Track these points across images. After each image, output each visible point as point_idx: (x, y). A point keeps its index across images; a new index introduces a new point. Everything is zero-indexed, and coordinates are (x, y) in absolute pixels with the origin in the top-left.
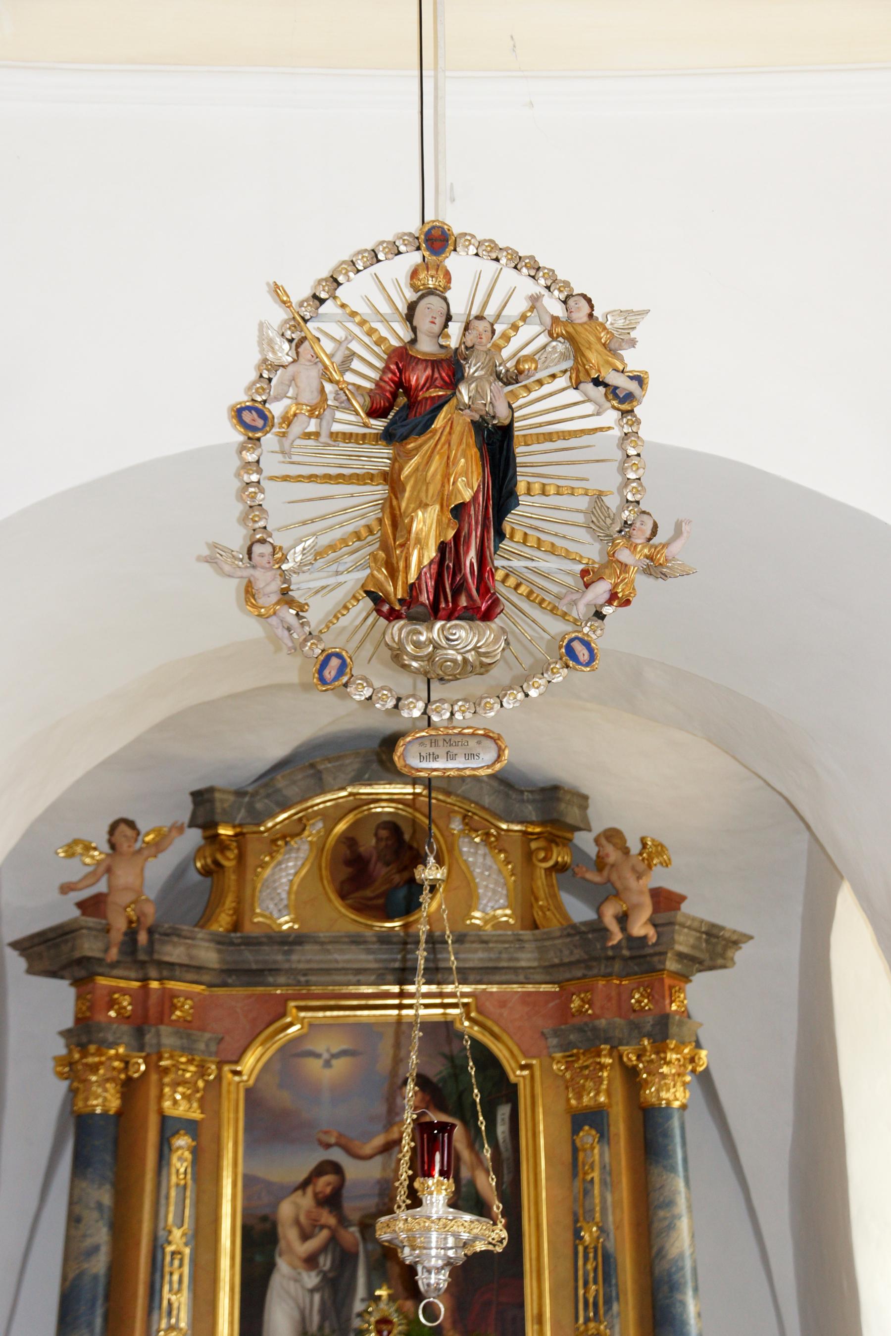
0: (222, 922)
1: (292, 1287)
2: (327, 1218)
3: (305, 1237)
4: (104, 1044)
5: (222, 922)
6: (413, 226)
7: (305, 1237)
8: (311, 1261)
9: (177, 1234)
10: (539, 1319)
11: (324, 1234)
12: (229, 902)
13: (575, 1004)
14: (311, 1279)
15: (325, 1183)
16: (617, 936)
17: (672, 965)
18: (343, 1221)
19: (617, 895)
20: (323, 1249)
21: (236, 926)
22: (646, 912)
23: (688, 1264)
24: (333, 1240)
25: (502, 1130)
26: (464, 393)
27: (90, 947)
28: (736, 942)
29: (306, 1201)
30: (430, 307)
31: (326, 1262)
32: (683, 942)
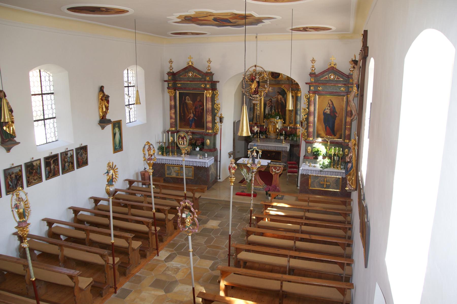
1: (268, 108)
3: (269, 104)
6: (254, 65)
7: (269, 104)
8: (269, 106)
10: (287, 112)
14: (269, 108)
15: (270, 100)
16: (294, 82)
18: (272, 103)
20: (270, 105)
23: (299, 109)
24: (271, 105)
25: (285, 97)
28: (305, 83)
29: (269, 102)
31: (270, 106)
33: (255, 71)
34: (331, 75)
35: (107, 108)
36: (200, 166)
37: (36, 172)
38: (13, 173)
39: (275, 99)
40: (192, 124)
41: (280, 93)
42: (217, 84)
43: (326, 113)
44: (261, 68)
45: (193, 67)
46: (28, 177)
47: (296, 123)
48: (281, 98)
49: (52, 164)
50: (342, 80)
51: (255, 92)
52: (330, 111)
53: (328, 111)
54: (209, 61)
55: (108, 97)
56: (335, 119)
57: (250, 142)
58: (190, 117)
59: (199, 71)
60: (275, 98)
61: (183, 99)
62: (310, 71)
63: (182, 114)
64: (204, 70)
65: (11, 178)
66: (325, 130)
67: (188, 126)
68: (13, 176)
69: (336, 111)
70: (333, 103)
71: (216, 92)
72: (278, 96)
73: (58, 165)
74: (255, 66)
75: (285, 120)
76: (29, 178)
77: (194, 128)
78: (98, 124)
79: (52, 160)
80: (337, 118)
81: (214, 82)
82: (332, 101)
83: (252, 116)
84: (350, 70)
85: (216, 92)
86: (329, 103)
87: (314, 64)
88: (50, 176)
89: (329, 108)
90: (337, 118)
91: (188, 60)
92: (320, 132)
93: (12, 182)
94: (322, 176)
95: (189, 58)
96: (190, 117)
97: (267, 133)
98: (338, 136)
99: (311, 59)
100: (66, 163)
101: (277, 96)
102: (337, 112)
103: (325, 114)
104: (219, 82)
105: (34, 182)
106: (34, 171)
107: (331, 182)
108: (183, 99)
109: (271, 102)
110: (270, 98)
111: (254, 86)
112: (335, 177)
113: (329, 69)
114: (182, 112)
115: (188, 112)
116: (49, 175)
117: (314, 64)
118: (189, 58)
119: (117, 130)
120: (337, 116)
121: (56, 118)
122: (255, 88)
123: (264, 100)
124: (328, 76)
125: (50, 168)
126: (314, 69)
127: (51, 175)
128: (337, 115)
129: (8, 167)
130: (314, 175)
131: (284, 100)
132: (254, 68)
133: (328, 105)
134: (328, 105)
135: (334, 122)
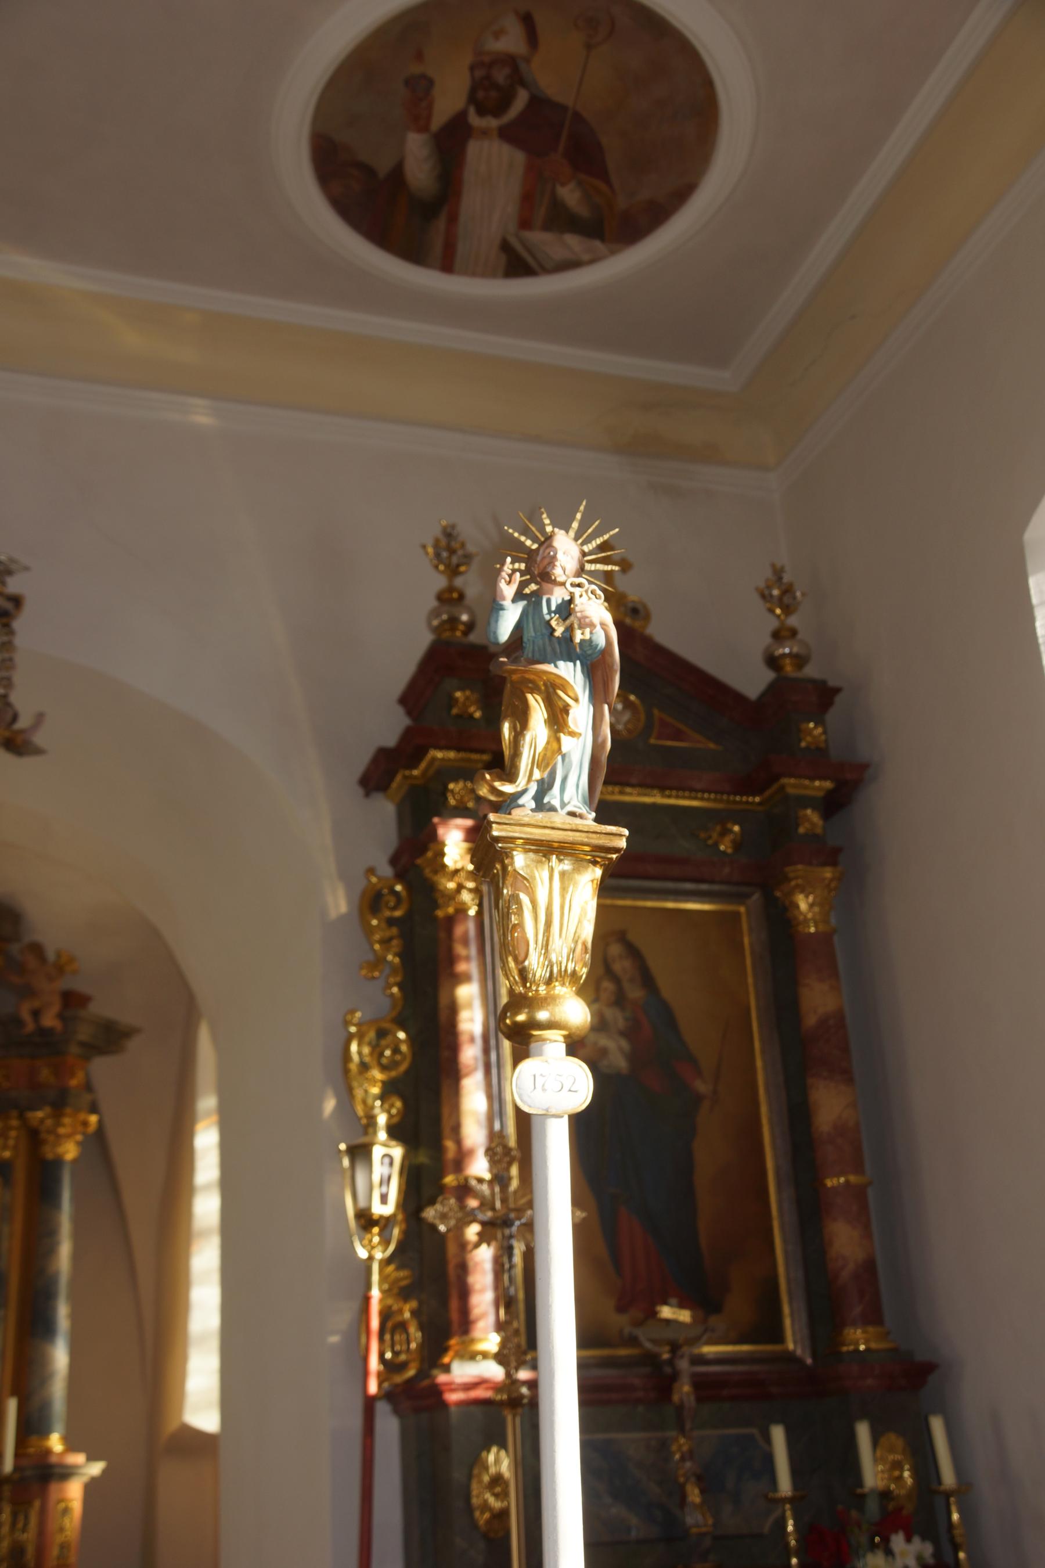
16: (30, 1027)
17: (74, 1050)
22: (55, 1008)
32: (84, 1033)
50: (712, 746)
52: (624, 1044)
82: (633, 952)
120: (698, 1099)
126: (465, 618)
128: (702, 1087)
133: (608, 985)
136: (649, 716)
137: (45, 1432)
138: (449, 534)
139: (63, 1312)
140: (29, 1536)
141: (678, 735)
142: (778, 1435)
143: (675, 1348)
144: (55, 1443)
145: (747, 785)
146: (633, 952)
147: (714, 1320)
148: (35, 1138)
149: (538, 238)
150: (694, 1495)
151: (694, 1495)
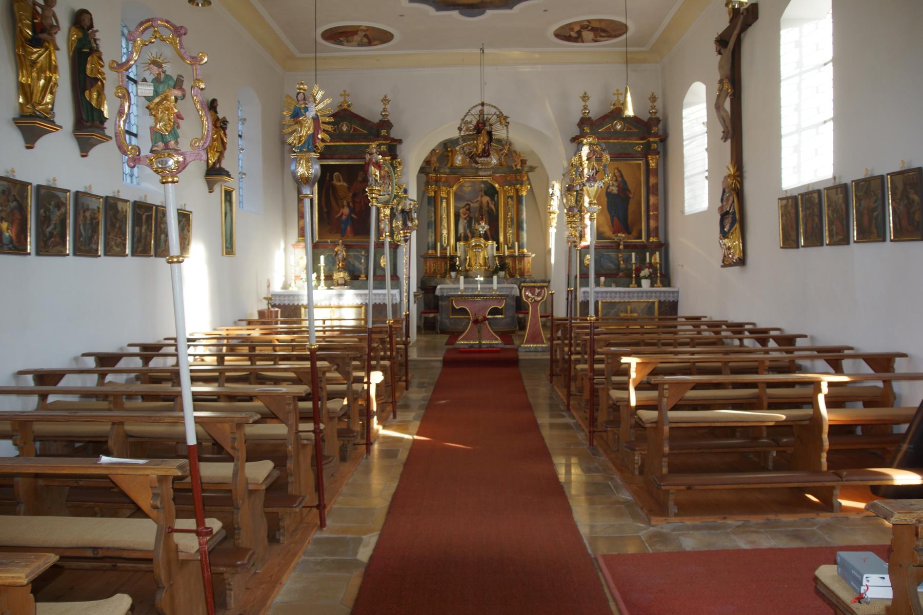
0: (449, 165)
2: (468, 212)
3: (464, 215)
4: (431, 186)
5: (449, 165)
6: (480, 102)
7: (464, 215)
8: (465, 219)
9: (444, 215)
11: (467, 215)
12: (450, 161)
13: (508, 178)
14: (466, 221)
15: (467, 207)
19: (515, 161)
20: (468, 216)
21: (452, 166)
24: (469, 216)
25: (496, 198)
26: (486, 128)
27: (428, 170)
29: (464, 209)
30: (482, 116)
31: (468, 219)
32: (526, 169)
33: (482, 113)
34: (616, 124)
35: (224, 144)
36: (380, 303)
37: (120, 228)
38: (88, 209)
39: (477, 205)
40: (346, 229)
41: (486, 194)
42: (398, 147)
43: (610, 192)
44: (495, 107)
45: (350, 112)
46: (107, 233)
47: (520, 247)
48: (488, 202)
49: (144, 224)
51: (484, 150)
53: (614, 190)
54: (385, 100)
55: (225, 122)
56: (628, 204)
57: (436, 287)
58: (342, 214)
59: (362, 121)
60: (478, 201)
61: (328, 178)
62: (582, 115)
63: (325, 210)
64: (376, 119)
65: (85, 218)
66: (610, 224)
67: (337, 233)
68: (88, 214)
69: (627, 187)
70: (623, 173)
71: (396, 162)
72: (481, 200)
73: (151, 231)
74: (483, 104)
75: (498, 243)
76: (109, 234)
77: (350, 235)
78: (205, 176)
79: (146, 214)
80: (631, 201)
81: (394, 140)
82: (619, 171)
83: (433, 238)
84: (650, 113)
85: (396, 162)
86: (615, 175)
87: (587, 103)
88: (140, 249)
89: (616, 184)
90: (630, 202)
91: (342, 99)
92: (601, 229)
93: (84, 229)
94: (622, 301)
95: (341, 95)
96: (342, 214)
97: (468, 268)
98: (635, 233)
99: (582, 94)
100: (161, 235)
101: (479, 198)
102: (629, 191)
103: (609, 194)
104: (400, 141)
105: (115, 248)
106: (117, 225)
107: (640, 311)
108: (328, 178)
109: (468, 210)
110: (466, 203)
111: (483, 139)
112: (646, 301)
113: (612, 112)
114: (323, 204)
115: (337, 203)
116: (138, 247)
117: (587, 103)
118: (341, 95)
119: (228, 204)
120: (630, 198)
121: (138, 136)
122: (484, 145)
123: (455, 207)
124: (612, 125)
125: (141, 231)
127: (140, 249)
128: (631, 196)
129: (82, 190)
130: (608, 301)
131: (495, 205)
132: (480, 108)
133: (614, 178)
134: (614, 178)
135: (626, 209)
136: (625, 125)
137: (523, 248)
138: (585, 94)
139: (525, 226)
140: (522, 266)
141: (630, 129)
142: (633, 254)
143: (620, 240)
144: (525, 250)
145: (642, 139)
146: (619, 171)
147: (630, 236)
148: (517, 191)
149: (599, 39)
150: (622, 262)
151: (622, 262)
